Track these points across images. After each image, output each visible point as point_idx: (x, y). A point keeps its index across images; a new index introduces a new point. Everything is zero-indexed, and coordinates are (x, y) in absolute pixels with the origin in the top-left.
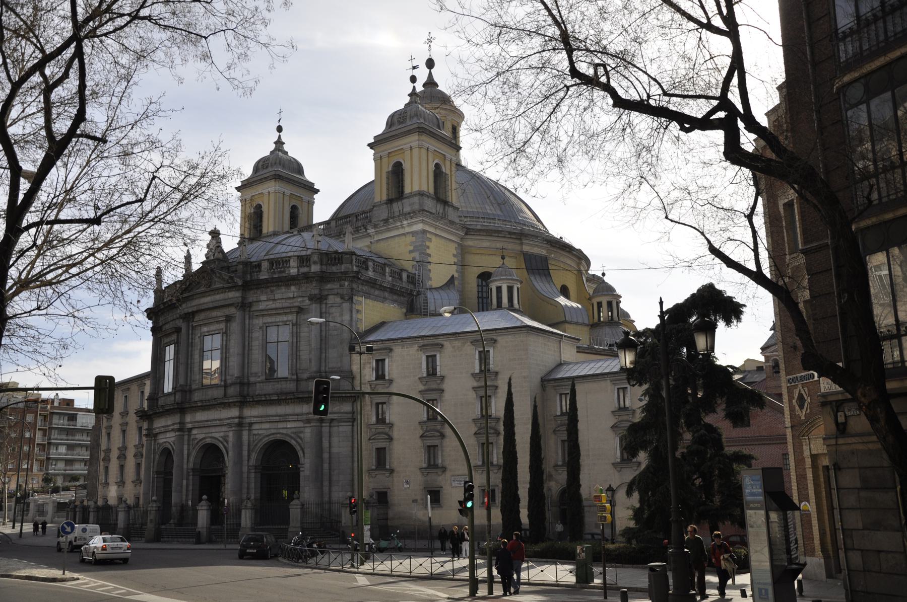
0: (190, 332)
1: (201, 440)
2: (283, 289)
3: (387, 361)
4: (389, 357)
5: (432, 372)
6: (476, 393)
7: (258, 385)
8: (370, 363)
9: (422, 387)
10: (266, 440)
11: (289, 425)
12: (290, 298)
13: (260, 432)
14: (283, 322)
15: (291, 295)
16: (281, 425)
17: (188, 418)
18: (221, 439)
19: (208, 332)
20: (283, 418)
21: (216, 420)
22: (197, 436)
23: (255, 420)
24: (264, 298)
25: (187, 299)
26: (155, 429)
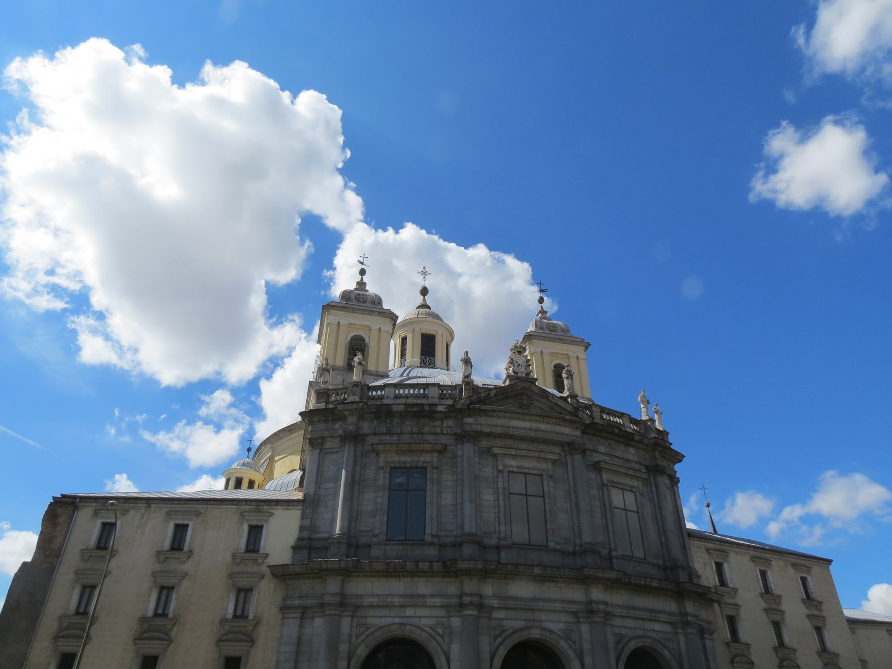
0: (477, 459)
1: (515, 631)
2: (622, 447)
3: (726, 566)
4: (726, 561)
5: (767, 590)
6: (810, 621)
7: (614, 560)
8: (711, 564)
9: (764, 605)
10: (633, 645)
11: (657, 627)
12: (629, 461)
13: (624, 631)
14: (630, 486)
15: (631, 458)
16: (649, 625)
17: (488, 589)
18: (561, 634)
19: (518, 467)
20: (653, 615)
21: (555, 601)
22: (507, 624)
23: (618, 611)
24: (602, 449)
25: (483, 413)
26: (361, 596)
